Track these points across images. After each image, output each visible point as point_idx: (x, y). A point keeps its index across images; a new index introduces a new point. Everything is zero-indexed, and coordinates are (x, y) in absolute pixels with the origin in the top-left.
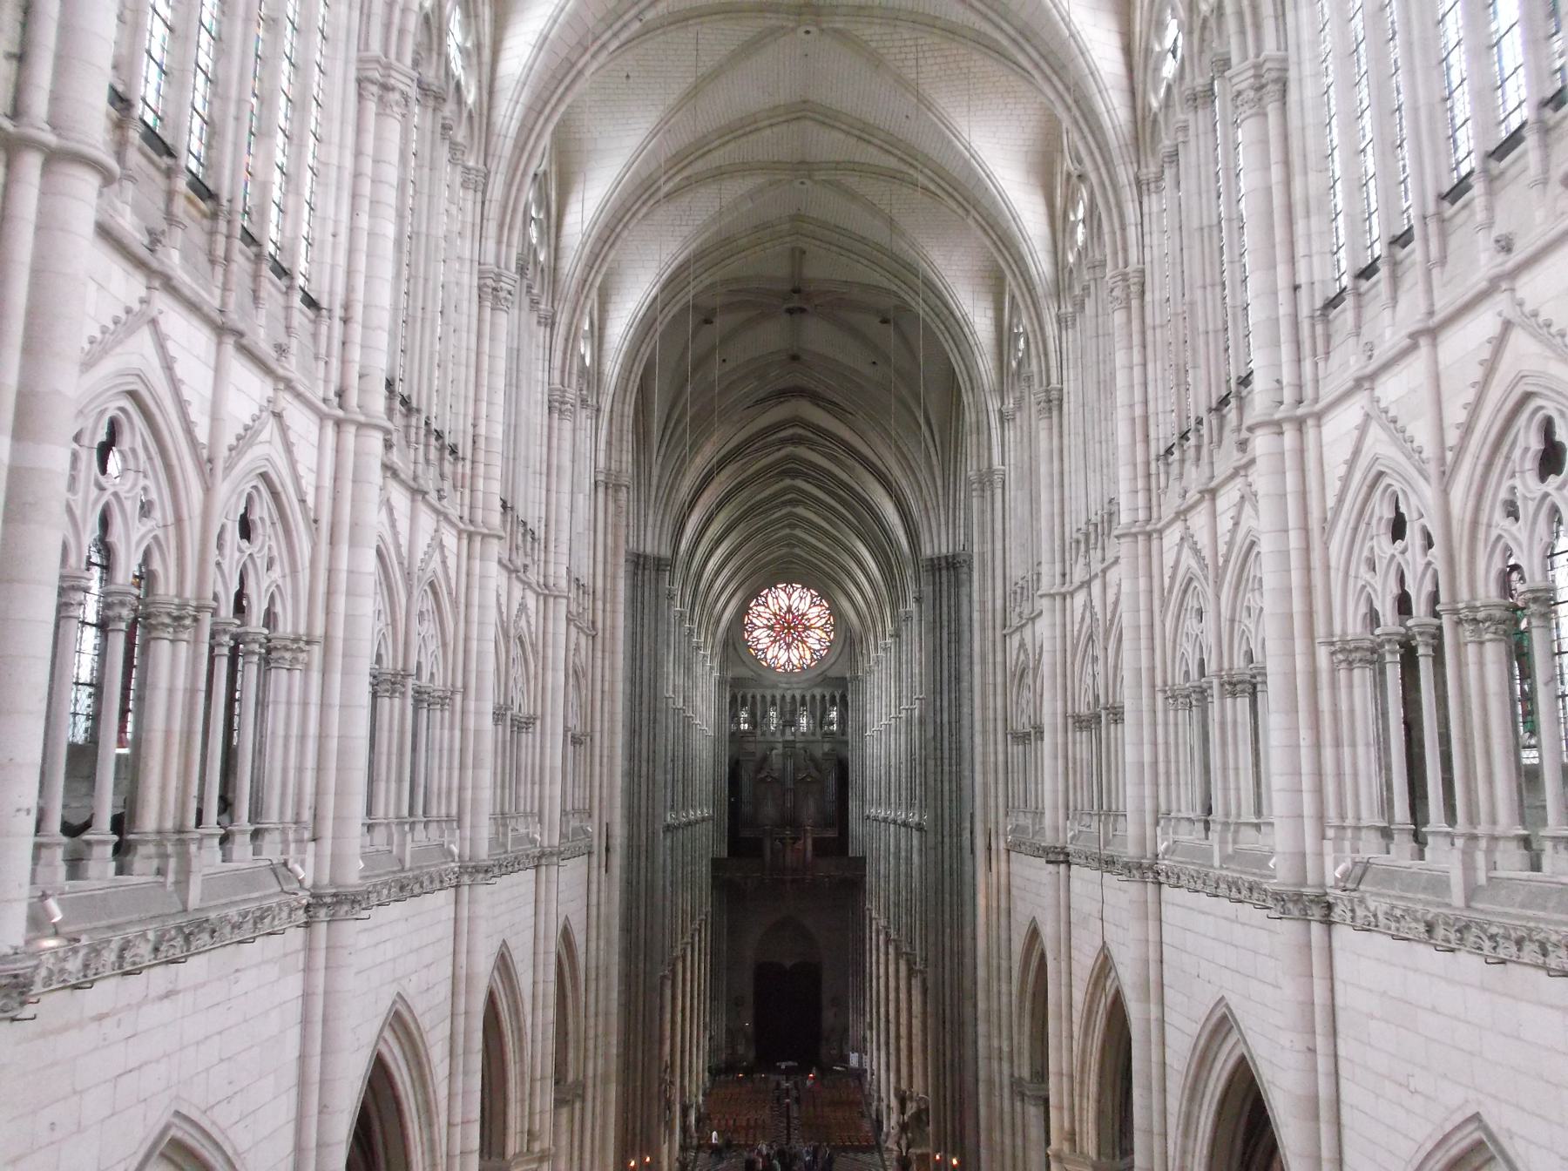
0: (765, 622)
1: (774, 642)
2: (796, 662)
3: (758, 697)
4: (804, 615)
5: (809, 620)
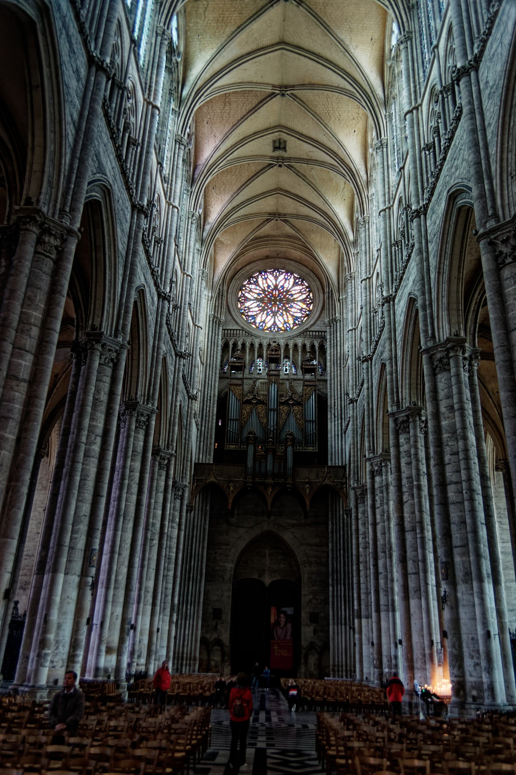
0: (256, 296)
1: (262, 310)
2: (281, 326)
3: (248, 345)
4: (288, 291)
5: (292, 295)
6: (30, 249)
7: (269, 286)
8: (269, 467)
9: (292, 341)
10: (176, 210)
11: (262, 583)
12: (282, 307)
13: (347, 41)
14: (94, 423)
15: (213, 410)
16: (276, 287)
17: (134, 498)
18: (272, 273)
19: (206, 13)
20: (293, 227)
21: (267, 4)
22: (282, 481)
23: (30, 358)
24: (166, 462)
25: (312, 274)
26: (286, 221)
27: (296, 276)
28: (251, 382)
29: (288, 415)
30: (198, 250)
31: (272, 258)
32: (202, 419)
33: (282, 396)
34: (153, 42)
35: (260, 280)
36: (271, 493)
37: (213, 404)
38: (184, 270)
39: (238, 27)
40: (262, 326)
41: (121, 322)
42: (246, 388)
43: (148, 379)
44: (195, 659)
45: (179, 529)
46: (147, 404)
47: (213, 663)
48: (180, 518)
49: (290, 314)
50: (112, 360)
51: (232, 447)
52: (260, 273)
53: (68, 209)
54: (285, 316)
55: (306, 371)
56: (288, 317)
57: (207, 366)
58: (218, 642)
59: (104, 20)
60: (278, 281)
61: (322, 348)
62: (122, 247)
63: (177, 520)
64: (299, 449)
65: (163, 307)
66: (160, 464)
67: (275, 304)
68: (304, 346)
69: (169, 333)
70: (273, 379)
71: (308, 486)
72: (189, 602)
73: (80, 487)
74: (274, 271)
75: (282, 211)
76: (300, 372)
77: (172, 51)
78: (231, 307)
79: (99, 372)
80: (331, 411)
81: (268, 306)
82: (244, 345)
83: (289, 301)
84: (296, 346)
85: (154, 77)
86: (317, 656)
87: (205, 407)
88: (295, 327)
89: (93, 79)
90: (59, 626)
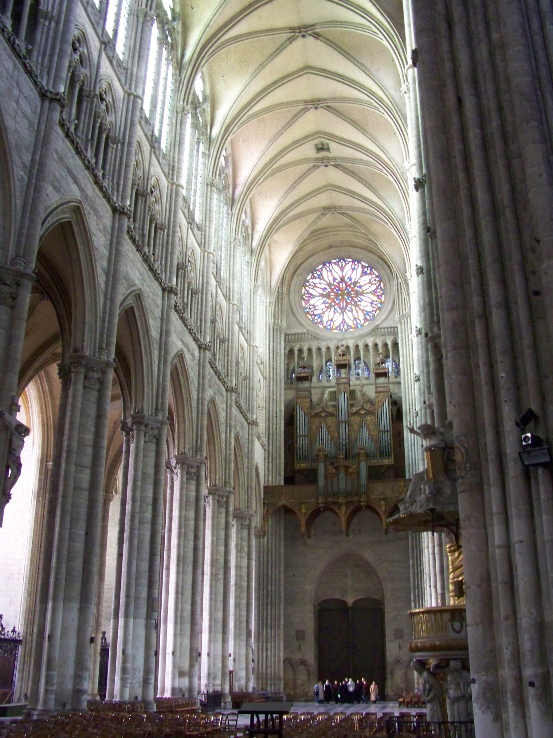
0: (321, 291)
2: (350, 323)
3: (314, 350)
4: (355, 283)
5: (360, 287)
6: (80, 387)
7: (334, 279)
8: (342, 485)
9: (362, 341)
10: (212, 255)
11: (345, 603)
12: (351, 301)
13: (368, 64)
14: (145, 494)
15: (280, 427)
16: (342, 280)
17: (191, 543)
18: (337, 264)
19: (229, 56)
20: (351, 217)
21: (286, 42)
22: (356, 499)
23: (88, 472)
24: (225, 499)
25: (381, 261)
26: (343, 214)
27: (364, 264)
28: (319, 391)
29: (360, 426)
30: (248, 262)
31: (337, 247)
32: (269, 439)
33: (352, 405)
34: (174, 122)
35: (324, 272)
36: (345, 512)
37: (280, 420)
38: (229, 300)
39: (261, 65)
40: (330, 325)
41: (160, 400)
42: (315, 398)
43: (195, 432)
44: (279, 679)
45: (249, 558)
46: (196, 456)
47: (299, 682)
48: (249, 547)
49: (360, 309)
50: (155, 436)
51: (303, 466)
52: (324, 265)
53: (104, 347)
54: (354, 311)
55: (378, 375)
56: (357, 313)
57: (270, 380)
58: (303, 662)
59: (124, 167)
60: (345, 271)
61: (396, 345)
62: (155, 334)
63: (246, 550)
64: (375, 462)
65: (204, 357)
66: (218, 501)
67: (343, 298)
68: (376, 345)
69: (216, 374)
70: (342, 387)
71: (383, 502)
72: (269, 626)
73: (138, 549)
74: (340, 260)
75: (337, 204)
76: (373, 376)
77: (196, 105)
78: (294, 307)
79: (144, 449)
80: (407, 419)
81: (335, 302)
82: (310, 350)
83: (357, 294)
84: (367, 346)
85: (176, 156)
86: (403, 671)
87: (271, 425)
88: (367, 323)
89: (117, 224)
90: (134, 657)
